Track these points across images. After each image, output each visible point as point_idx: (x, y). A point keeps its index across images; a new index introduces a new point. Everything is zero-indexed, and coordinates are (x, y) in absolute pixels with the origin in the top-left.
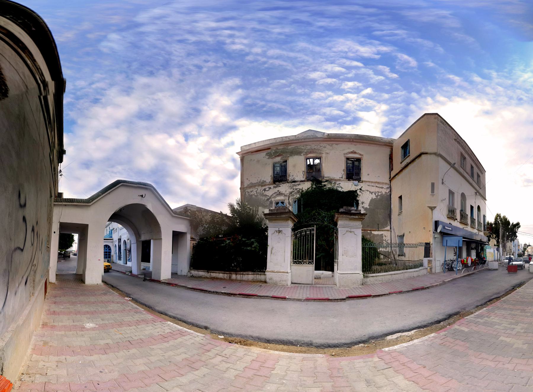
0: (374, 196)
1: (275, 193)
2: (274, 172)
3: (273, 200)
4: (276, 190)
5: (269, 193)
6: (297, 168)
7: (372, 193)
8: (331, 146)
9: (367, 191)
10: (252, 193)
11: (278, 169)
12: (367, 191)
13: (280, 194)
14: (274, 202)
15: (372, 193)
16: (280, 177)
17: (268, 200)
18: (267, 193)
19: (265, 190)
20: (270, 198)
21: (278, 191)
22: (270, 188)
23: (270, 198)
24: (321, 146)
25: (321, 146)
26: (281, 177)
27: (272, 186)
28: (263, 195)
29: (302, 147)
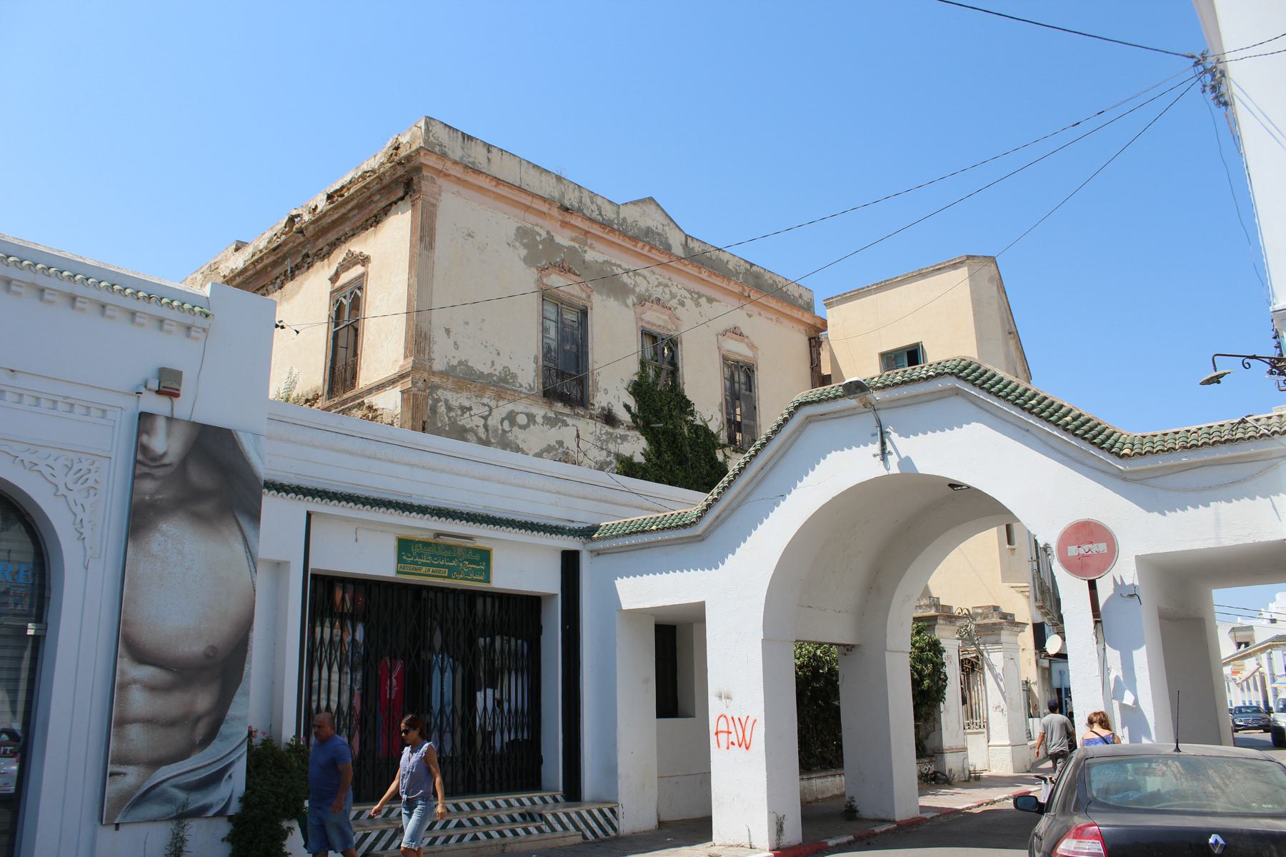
4: (553, 435)
11: (553, 333)
19: (511, 417)
25: (673, 296)
27: (540, 411)
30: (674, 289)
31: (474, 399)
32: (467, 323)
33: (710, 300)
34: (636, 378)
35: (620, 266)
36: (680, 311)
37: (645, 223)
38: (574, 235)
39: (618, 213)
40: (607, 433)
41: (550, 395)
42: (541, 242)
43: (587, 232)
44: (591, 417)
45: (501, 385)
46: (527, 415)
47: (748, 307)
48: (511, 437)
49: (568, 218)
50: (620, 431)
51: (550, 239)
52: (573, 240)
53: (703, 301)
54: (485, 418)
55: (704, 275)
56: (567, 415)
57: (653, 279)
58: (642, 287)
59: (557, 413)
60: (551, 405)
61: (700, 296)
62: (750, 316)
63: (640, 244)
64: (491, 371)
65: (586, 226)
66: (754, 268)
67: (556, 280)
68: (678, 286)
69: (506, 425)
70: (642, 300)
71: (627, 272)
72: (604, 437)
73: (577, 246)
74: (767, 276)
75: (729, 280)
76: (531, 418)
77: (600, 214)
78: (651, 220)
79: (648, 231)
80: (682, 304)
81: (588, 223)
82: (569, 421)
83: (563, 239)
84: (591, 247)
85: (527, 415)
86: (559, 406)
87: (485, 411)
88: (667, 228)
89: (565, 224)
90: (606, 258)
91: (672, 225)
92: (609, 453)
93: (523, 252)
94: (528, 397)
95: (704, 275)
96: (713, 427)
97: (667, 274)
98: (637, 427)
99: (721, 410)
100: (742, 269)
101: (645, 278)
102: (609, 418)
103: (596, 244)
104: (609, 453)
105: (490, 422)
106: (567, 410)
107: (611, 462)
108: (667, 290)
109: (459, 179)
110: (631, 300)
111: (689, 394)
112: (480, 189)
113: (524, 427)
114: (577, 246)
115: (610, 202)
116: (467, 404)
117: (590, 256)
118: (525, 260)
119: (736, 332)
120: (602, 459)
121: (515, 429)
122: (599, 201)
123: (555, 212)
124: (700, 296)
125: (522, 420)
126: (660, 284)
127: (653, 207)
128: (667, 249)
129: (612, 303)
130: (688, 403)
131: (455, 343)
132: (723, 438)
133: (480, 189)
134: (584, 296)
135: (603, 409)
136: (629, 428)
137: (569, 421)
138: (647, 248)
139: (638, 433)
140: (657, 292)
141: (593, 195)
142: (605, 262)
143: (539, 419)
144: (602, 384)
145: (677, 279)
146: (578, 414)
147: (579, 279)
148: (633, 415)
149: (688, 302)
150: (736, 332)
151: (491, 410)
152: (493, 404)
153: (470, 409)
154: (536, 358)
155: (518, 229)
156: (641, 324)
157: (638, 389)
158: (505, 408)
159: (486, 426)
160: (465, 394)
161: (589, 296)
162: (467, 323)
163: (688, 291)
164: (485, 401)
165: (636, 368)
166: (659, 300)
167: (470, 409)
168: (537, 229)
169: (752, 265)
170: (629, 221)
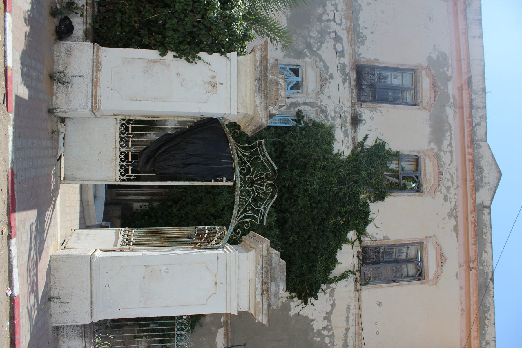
0: (317, 326)
1: (326, 67)
2: (386, 69)
3: (307, 60)
4: (334, 70)
5: (327, 52)
6: (394, 128)
7: (327, 318)
8: (450, 215)
9: (333, 306)
10: (329, 7)
12: (333, 306)
13: (324, 79)
14: (299, 62)
15: (327, 318)
16: (371, 85)
17: (309, 46)
18: (329, 44)
19: (338, 39)
20: (314, 53)
21: (331, 77)
22: (341, 54)
23: (314, 53)
24: (448, 189)
25: (448, 189)
26: (372, 86)
27: (346, 60)
28: (323, 33)
29: (446, 143)
30: (452, 190)
31: (343, 13)
32: (383, 12)
33: (456, 229)
34: (387, 148)
35: (451, 139)
36: (440, 197)
37: (484, 164)
38: (457, 98)
39: (481, 140)
40: (346, 117)
41: (360, 70)
42: (444, 71)
43: (462, 107)
44: (353, 104)
45: (356, 34)
46: (343, 51)
47: (463, 273)
48: (327, 38)
49: (465, 88)
50: (350, 130)
51: (449, 79)
52: (454, 97)
53: (453, 222)
54: (334, 20)
55: (471, 218)
56: (350, 83)
57: (453, 171)
58: (446, 158)
59: (349, 74)
60: (352, 69)
61: (456, 217)
62: (457, 275)
63: (471, 150)
64: (361, 27)
65: (466, 103)
66: (491, 283)
67: (426, 84)
68: (456, 194)
69: (333, 35)
70: (437, 156)
71: (450, 145)
72: (343, 115)
73: (452, 100)
74: (490, 299)
75: (475, 244)
76: (341, 54)
77: (476, 125)
78: (489, 175)
79: (480, 169)
80: (446, 199)
81: (468, 103)
82: (347, 84)
83: (452, 88)
84: (455, 112)
85: (343, 51)
86: (354, 76)
87: (338, 21)
88: (487, 187)
89: (460, 89)
90: (452, 125)
91: (492, 192)
92: (333, 119)
93: (434, 56)
94: (353, 51)
95: (471, 218)
96: (370, 229)
97: (460, 183)
98: (355, 148)
99: (384, 238)
100: (487, 269)
101: (451, 161)
102: (356, 121)
103: (458, 116)
104: (333, 119)
105: (332, 23)
106: (353, 83)
107: (328, 120)
108: (449, 184)
109: (457, 11)
110: (433, 146)
111: (388, 200)
112: (457, 26)
113: (335, 48)
114: (452, 100)
115: (486, 133)
116: (339, 8)
117: (449, 111)
118: (430, 57)
119: (441, 261)
120: (329, 112)
121: (333, 42)
122: (483, 123)
123: (465, 77)
124: (456, 217)
125: (339, 47)
126: (452, 176)
127: (496, 175)
128: (476, 188)
129: (427, 130)
130: (382, 199)
131: (370, 3)
132: (366, 241)
133: (457, 26)
134: (425, 104)
135: (360, 115)
136: (353, 138)
137: (347, 84)
138: (471, 157)
139: (351, 147)
140: (446, 175)
141: (484, 117)
142: (450, 124)
143: (342, 60)
144: (375, 114)
145: (460, 191)
146: (352, 93)
147: (433, 98)
148: (362, 144)
149: (448, 207)
150: (441, 261)
151: (340, 24)
152: (343, 26)
153: (337, 11)
154: (377, 60)
155: (445, 54)
156: (422, 154)
157: (379, 153)
158: (344, 35)
159: (329, 20)
160: (344, 7)
161: (425, 109)
162: (383, 12)
163: (455, 208)
164: (344, 21)
165: (394, 149)
166: (441, 173)
167: (337, 11)
168: (450, 68)
169: (492, 279)
170: (481, 150)
